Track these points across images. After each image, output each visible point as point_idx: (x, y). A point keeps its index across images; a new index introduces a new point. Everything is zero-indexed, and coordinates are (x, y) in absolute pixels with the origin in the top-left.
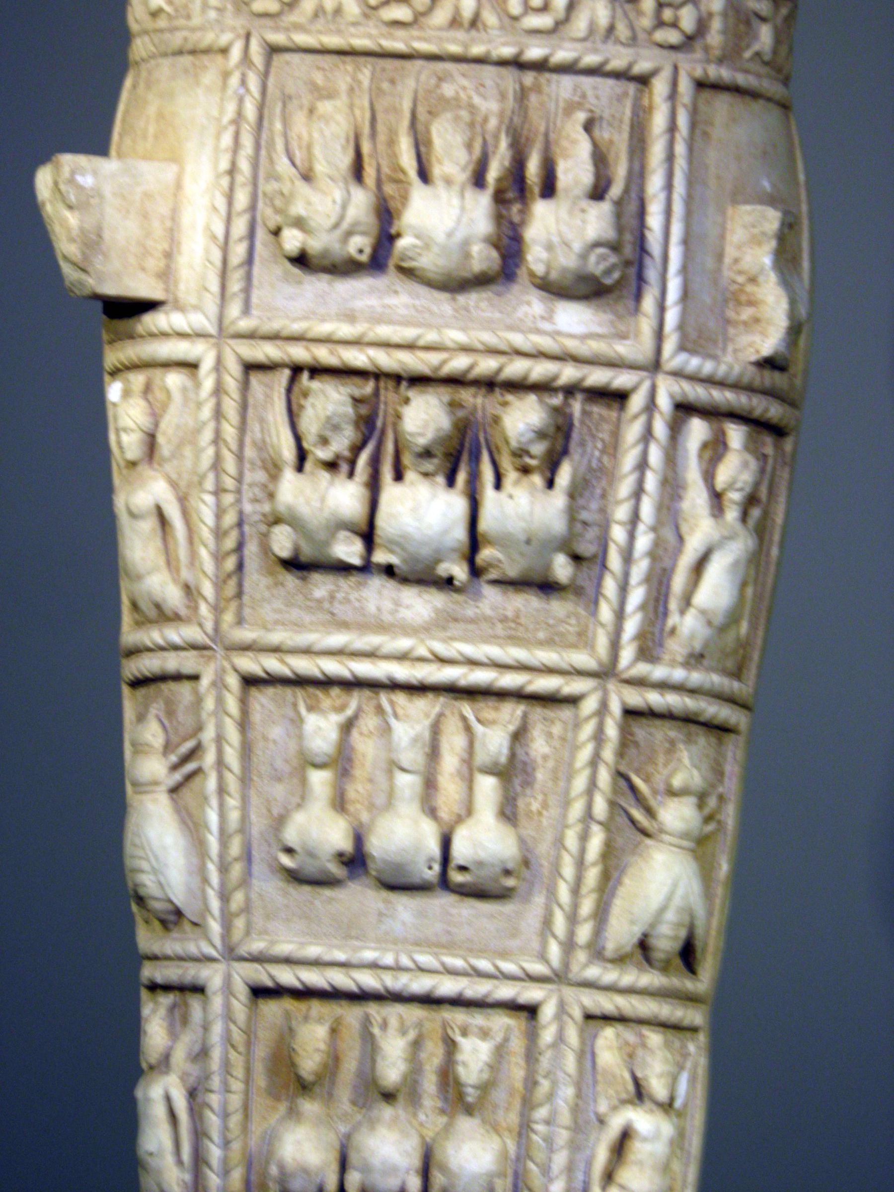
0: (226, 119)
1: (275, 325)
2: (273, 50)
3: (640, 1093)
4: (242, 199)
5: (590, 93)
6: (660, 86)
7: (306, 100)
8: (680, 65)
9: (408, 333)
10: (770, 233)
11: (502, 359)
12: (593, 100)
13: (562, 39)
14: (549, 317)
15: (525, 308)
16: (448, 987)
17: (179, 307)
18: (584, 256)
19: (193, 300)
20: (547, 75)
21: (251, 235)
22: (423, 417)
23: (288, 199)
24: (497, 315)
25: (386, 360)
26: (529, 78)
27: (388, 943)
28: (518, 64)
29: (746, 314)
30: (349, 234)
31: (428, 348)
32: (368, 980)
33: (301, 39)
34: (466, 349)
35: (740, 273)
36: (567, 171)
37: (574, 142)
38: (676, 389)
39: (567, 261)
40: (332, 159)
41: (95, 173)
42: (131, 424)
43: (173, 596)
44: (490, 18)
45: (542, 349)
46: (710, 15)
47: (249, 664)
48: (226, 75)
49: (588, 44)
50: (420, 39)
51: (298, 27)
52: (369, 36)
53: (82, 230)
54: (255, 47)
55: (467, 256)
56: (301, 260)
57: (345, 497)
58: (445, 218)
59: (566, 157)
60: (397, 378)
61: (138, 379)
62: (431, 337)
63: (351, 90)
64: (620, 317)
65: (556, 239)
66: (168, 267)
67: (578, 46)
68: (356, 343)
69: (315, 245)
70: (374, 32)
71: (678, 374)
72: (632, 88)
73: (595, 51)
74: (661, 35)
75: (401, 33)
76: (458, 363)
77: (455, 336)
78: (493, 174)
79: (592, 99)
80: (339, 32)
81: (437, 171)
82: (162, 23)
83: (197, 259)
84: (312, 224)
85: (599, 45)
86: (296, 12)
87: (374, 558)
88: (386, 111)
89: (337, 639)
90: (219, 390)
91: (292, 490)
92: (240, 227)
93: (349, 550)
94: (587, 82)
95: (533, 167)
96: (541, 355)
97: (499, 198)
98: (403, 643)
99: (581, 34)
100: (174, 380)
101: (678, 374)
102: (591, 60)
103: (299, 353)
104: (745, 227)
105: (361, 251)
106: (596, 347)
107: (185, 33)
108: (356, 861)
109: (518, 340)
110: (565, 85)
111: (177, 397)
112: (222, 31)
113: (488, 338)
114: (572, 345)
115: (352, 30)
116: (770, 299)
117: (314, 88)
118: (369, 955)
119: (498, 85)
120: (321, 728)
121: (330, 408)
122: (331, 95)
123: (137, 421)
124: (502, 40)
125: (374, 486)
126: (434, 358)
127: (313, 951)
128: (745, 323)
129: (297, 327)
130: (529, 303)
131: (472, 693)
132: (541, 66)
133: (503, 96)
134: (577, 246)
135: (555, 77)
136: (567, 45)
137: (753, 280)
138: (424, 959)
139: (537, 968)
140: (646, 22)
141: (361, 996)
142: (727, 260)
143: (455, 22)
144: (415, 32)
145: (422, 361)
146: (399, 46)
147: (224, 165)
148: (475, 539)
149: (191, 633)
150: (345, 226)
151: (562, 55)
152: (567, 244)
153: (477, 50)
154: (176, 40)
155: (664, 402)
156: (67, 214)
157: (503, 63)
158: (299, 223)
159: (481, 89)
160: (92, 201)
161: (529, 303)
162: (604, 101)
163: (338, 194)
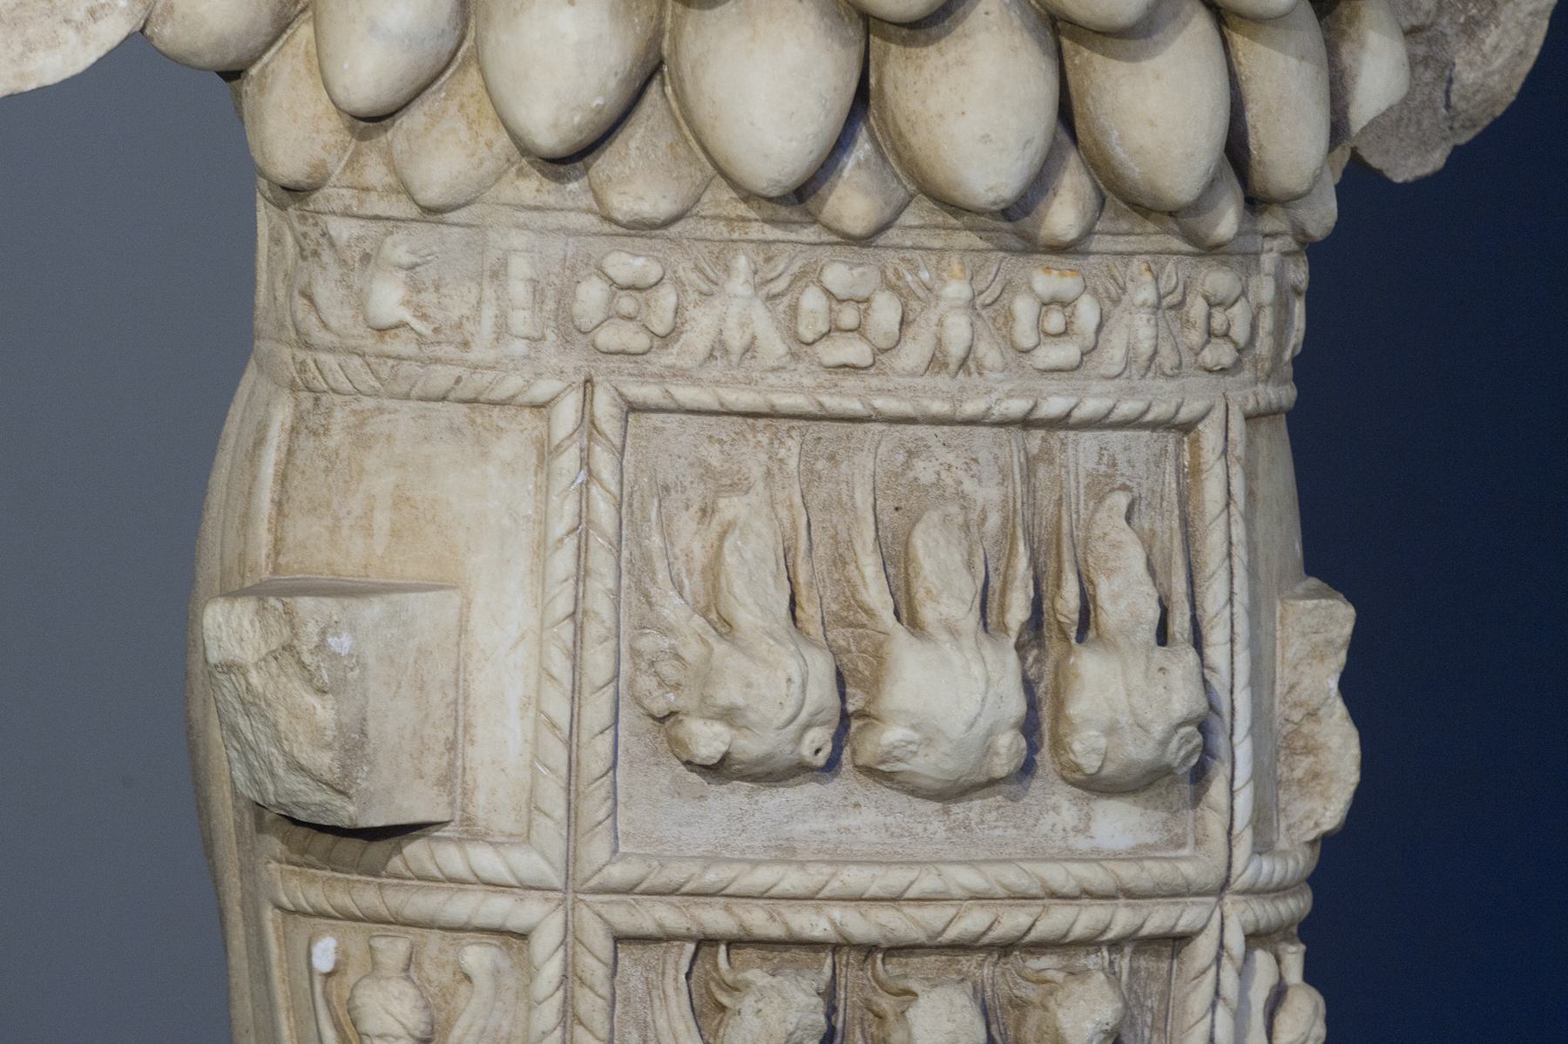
0: (560, 526)
1: (674, 874)
2: (633, 408)
5: (1121, 458)
6: (1210, 435)
7: (696, 494)
8: (1230, 394)
9: (895, 879)
10: (1340, 641)
11: (1035, 909)
12: (1127, 471)
13: (1088, 377)
14: (1083, 830)
15: (1050, 818)
17: (472, 833)
18: (1164, 743)
19: (506, 822)
20: (1062, 434)
23: (706, 675)
24: (1012, 832)
25: (859, 925)
26: (1036, 439)
28: (1026, 423)
29: (1303, 765)
30: (807, 727)
31: (921, 900)
33: (687, 394)
34: (978, 897)
35: (1296, 705)
36: (1115, 598)
37: (1117, 546)
38: (1250, 916)
39: (1139, 751)
40: (755, 600)
41: (353, 629)
42: (397, 1029)
44: (990, 354)
45: (1086, 885)
46: (1260, 307)
48: (546, 453)
49: (1121, 382)
50: (880, 391)
51: (679, 374)
52: (800, 388)
53: (340, 726)
54: (604, 406)
55: (988, 750)
56: (720, 770)
58: (949, 691)
59: (1110, 573)
60: (868, 950)
61: (393, 949)
62: (927, 882)
63: (769, 474)
64: (1174, 812)
65: (1125, 720)
66: (451, 764)
67: (1109, 386)
68: (809, 898)
69: (751, 747)
70: (807, 381)
71: (1251, 891)
72: (1171, 438)
73: (1132, 392)
74: (1209, 356)
75: (851, 382)
76: (973, 922)
77: (969, 878)
78: (1018, 613)
79: (1123, 467)
80: (750, 382)
81: (928, 614)
82: (399, 345)
84: (752, 716)
85: (1136, 382)
86: (675, 349)
88: (826, 508)
90: (570, 976)
92: (597, 710)
94: (1115, 438)
96: (1087, 894)
97: (1020, 647)
99: (1116, 370)
100: (478, 957)
101: (1251, 891)
102: (1128, 408)
103: (716, 919)
104: (1304, 634)
105: (817, 751)
106: (1153, 872)
107: (458, 371)
109: (1058, 876)
111: (483, 981)
112: (538, 375)
113: (1012, 877)
114: (1129, 874)
115: (772, 379)
116: (1335, 742)
117: (707, 472)
119: (996, 458)
121: (793, 1018)
122: (738, 486)
123: (409, 1025)
124: (1008, 387)
128: (1300, 781)
129: (713, 876)
130: (1056, 808)
132: (1062, 423)
133: (1004, 476)
134: (1158, 730)
135: (1071, 434)
136: (1097, 387)
137: (1312, 715)
140: (1196, 337)
142: (1279, 689)
143: (936, 362)
144: (874, 382)
145: (916, 923)
146: (854, 406)
147: (563, 605)
150: (803, 716)
151: (1091, 407)
152: (1143, 728)
153: (971, 408)
154: (441, 378)
155: (1235, 941)
156: (312, 700)
157: (1004, 423)
158: (729, 716)
159: (974, 467)
160: (350, 675)
161: (1055, 808)
162: (1141, 469)
163: (793, 667)
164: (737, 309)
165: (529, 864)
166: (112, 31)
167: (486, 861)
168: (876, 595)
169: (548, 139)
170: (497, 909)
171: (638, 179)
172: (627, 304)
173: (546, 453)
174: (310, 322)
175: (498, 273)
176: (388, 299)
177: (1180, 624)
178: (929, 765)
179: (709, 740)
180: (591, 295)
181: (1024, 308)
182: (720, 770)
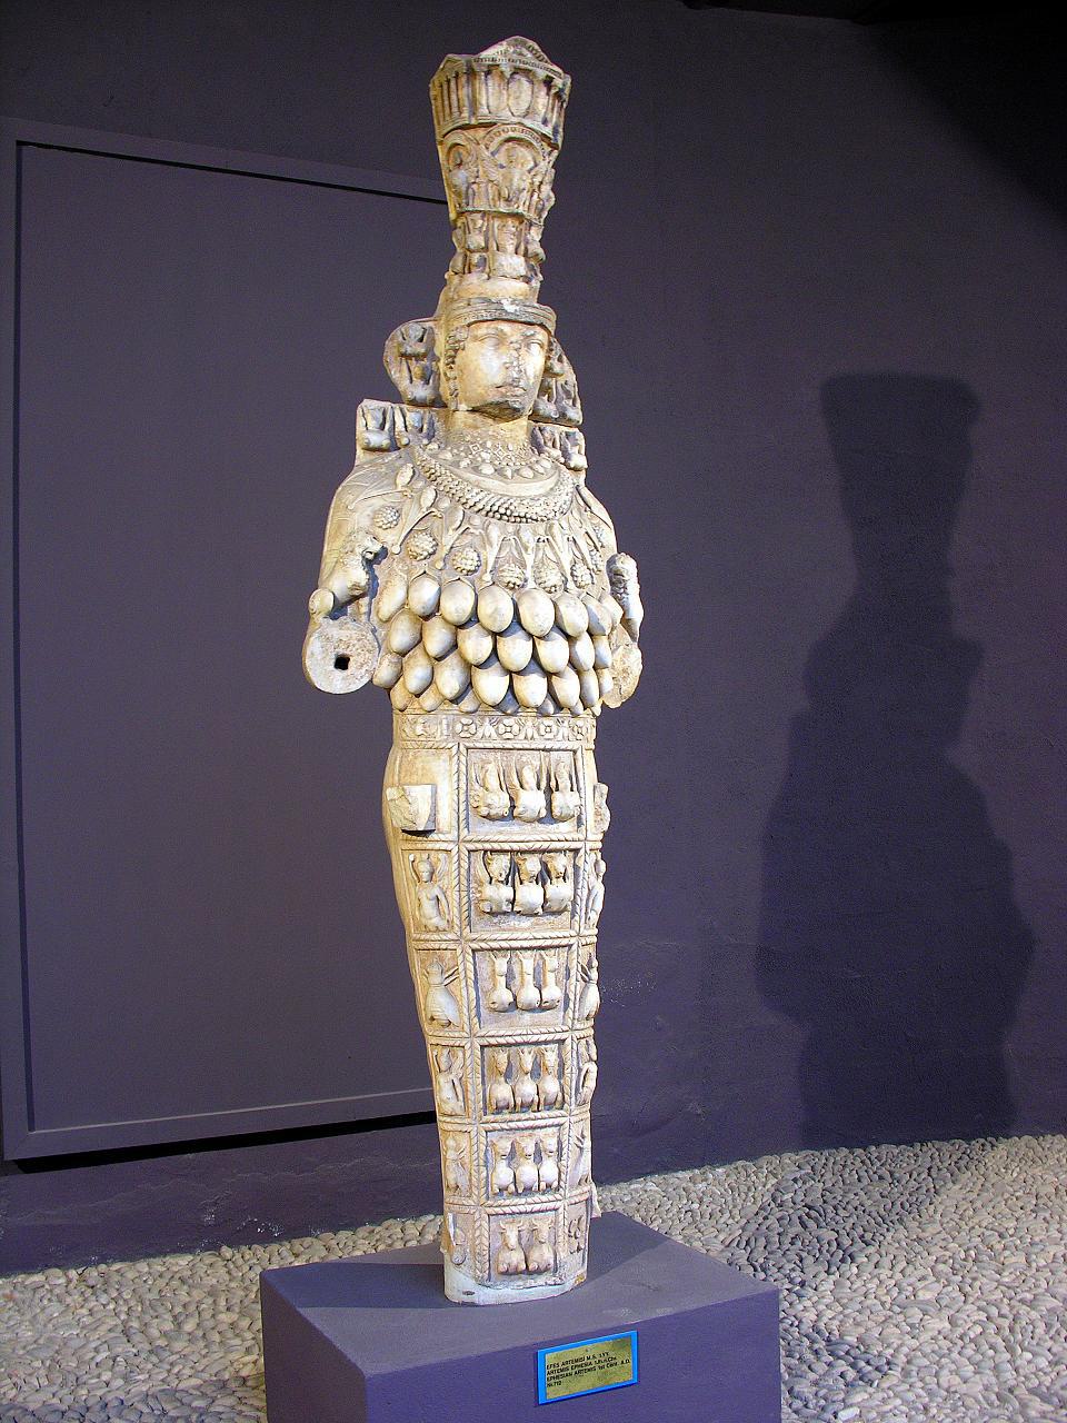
3: (591, 1059)
4: (463, 798)
16: (543, 1038)
19: (446, 829)
21: (467, 809)
22: (532, 865)
25: (515, 846)
27: (523, 1026)
32: (519, 1039)
33: (478, 745)
40: (493, 782)
43: (443, 924)
44: (536, 736)
47: (475, 946)
48: (451, 758)
51: (477, 741)
56: (488, 817)
57: (507, 892)
58: (532, 801)
61: (425, 856)
69: (493, 812)
76: (537, 845)
81: (525, 786)
83: (446, 817)
87: (513, 909)
89: (505, 936)
91: (489, 891)
92: (462, 807)
93: (505, 908)
95: (553, 784)
98: (526, 935)
100: (442, 856)
102: (563, 747)
103: (487, 846)
108: (514, 1005)
110: (554, 755)
118: (519, 1032)
120: (501, 964)
125: (514, 887)
126: (530, 845)
127: (501, 1033)
129: (487, 838)
131: (543, 948)
138: (535, 1031)
139: (565, 1028)
141: (517, 1044)
148: (545, 900)
149: (450, 936)
154: (430, 744)
164: (488, 729)
165: (450, 837)
166: (365, 680)
167: (442, 837)
168: (516, 782)
169: (449, 696)
170: (444, 846)
171: (468, 704)
172: (465, 728)
173: (451, 758)
174: (404, 735)
175: (441, 723)
176: (419, 729)
177: (575, 789)
178: (527, 815)
179: (484, 811)
180: (459, 727)
181: (542, 728)
182: (488, 817)
